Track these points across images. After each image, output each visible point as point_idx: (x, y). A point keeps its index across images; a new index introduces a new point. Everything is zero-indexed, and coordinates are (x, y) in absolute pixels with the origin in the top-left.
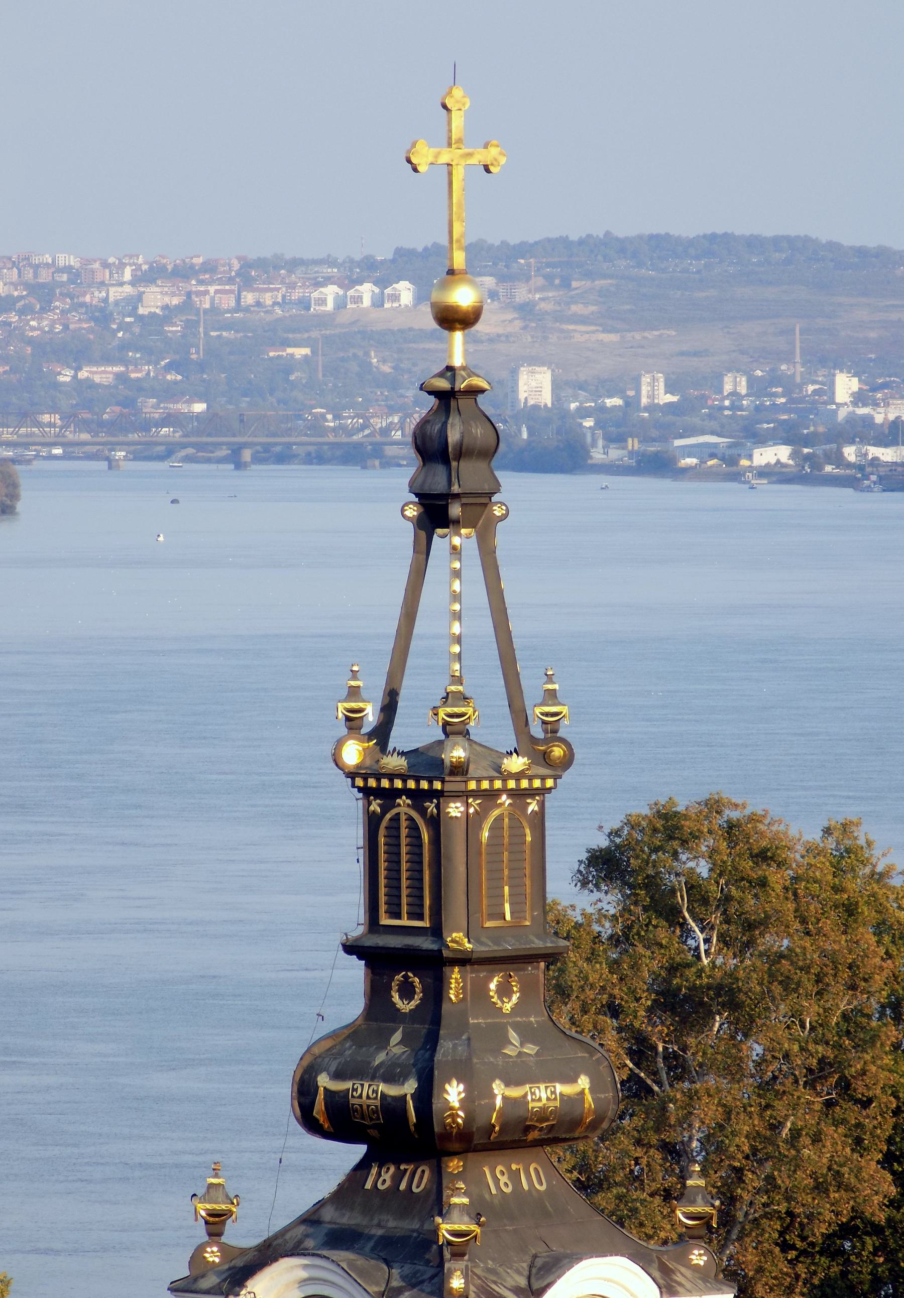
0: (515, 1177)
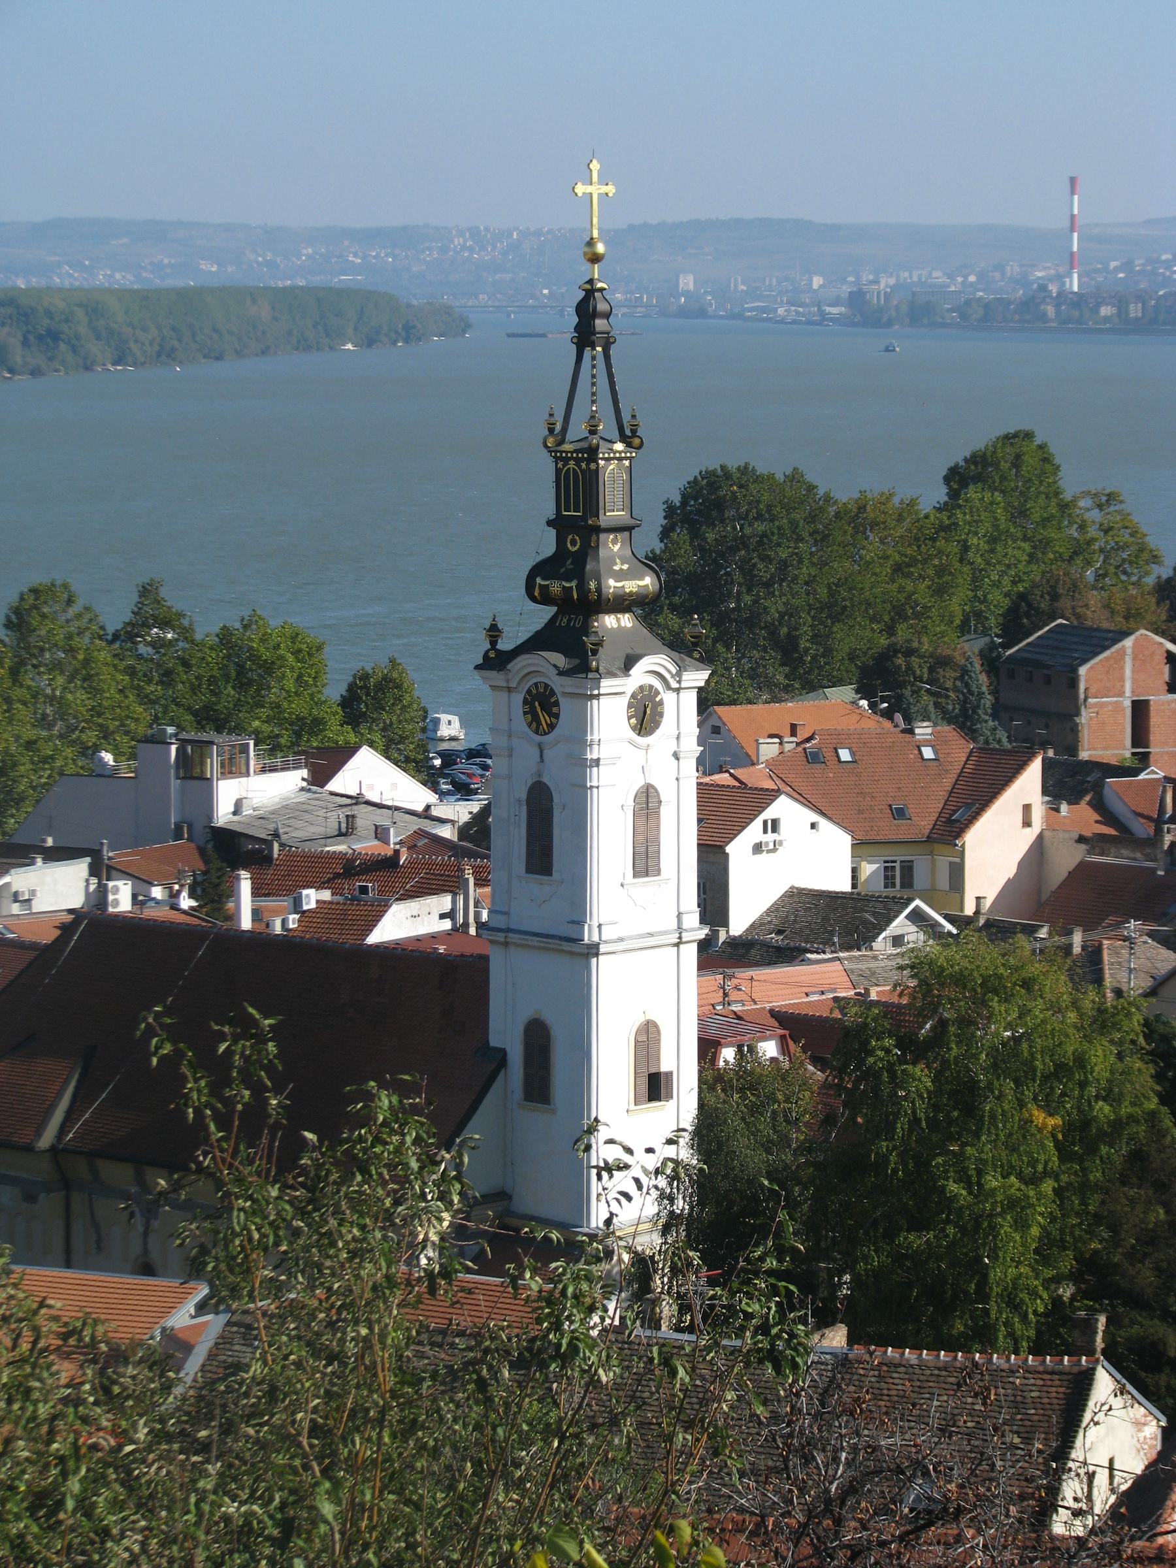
0: (618, 620)
